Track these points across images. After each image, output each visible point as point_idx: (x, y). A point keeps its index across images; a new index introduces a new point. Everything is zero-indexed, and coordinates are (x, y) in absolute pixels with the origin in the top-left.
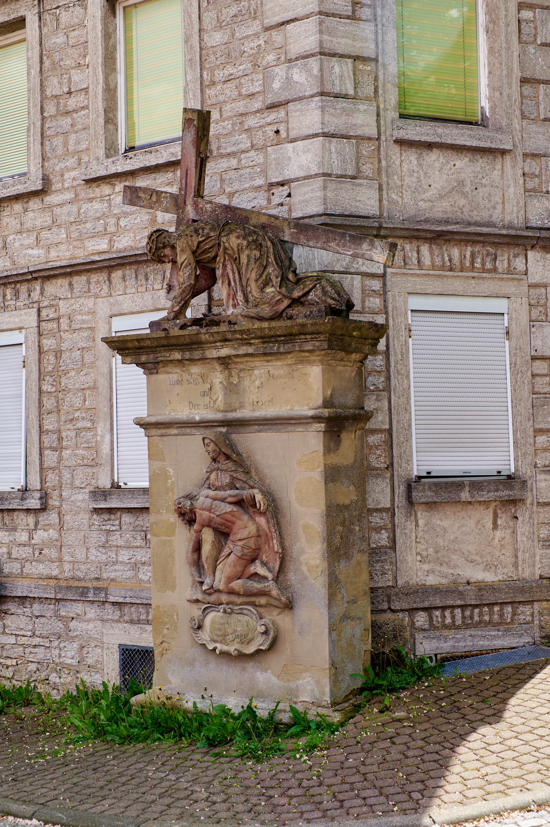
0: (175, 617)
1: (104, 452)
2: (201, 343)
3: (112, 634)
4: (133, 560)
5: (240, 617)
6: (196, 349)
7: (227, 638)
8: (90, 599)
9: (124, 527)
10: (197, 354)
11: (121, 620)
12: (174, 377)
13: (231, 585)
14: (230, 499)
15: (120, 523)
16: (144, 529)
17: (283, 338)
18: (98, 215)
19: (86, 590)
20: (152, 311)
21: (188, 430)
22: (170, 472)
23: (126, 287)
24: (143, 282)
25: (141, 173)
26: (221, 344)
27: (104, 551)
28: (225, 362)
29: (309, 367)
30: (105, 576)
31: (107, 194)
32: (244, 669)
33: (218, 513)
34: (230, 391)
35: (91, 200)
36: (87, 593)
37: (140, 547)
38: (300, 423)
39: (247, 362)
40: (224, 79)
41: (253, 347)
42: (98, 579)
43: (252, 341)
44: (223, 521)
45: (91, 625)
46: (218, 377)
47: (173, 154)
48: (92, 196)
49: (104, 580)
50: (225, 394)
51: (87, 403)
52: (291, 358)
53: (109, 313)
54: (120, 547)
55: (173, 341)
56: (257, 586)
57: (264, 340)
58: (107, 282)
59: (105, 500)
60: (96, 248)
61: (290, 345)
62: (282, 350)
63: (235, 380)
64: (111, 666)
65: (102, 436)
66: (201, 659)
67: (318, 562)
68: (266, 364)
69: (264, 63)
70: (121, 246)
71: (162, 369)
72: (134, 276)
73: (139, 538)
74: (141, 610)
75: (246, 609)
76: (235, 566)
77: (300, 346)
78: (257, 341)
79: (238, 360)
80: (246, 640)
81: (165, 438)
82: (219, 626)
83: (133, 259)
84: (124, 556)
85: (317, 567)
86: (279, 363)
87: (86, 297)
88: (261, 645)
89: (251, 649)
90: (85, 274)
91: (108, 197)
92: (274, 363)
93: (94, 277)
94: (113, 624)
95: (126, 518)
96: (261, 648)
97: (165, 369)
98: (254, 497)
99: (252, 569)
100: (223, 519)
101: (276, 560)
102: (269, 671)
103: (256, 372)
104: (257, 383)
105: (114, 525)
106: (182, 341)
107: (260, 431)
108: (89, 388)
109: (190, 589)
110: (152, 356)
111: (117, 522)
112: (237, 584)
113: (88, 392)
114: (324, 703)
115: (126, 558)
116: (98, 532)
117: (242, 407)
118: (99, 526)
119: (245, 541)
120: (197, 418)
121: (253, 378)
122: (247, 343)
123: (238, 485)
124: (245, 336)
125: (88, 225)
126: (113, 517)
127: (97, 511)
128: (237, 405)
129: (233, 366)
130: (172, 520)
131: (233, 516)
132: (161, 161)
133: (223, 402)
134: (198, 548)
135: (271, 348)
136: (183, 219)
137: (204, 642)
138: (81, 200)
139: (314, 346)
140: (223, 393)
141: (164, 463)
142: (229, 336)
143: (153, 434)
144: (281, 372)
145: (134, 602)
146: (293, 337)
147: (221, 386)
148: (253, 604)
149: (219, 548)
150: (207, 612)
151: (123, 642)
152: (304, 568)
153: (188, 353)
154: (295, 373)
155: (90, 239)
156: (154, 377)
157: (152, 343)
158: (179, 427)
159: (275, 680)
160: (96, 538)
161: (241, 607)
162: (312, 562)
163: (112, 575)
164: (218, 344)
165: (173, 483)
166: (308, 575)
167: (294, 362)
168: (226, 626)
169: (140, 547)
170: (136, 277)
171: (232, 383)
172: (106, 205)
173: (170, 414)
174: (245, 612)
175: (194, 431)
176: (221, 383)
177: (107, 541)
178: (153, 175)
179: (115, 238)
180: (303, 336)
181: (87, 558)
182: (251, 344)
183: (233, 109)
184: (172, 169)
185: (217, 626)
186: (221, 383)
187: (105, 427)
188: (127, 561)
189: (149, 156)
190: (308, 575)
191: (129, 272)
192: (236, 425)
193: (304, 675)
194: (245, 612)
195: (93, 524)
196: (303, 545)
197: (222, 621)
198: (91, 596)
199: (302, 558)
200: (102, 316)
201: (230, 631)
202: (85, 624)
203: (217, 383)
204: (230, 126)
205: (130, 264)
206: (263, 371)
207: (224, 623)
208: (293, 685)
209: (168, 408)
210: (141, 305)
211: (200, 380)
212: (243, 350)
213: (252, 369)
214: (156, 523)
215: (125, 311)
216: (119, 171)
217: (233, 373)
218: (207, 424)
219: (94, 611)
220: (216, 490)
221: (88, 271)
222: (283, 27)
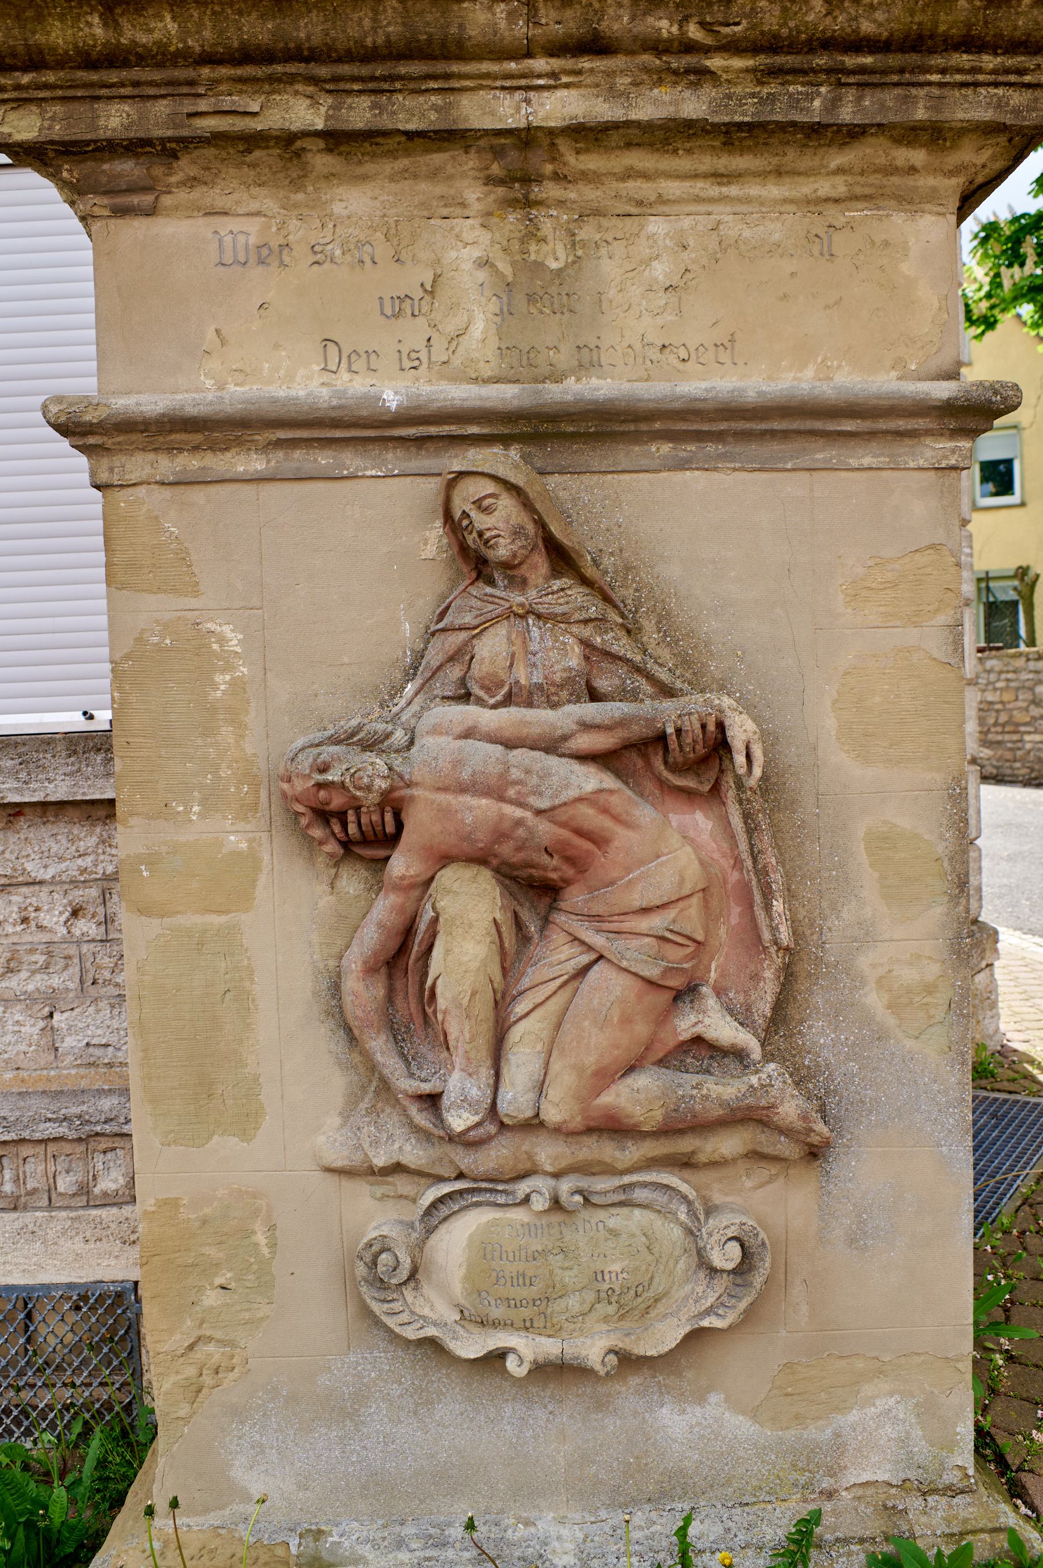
0: (261, 1238)
2: (456, 50)
5: (616, 1219)
6: (415, 86)
7: (558, 1306)
10: (412, 112)
12: (244, 231)
13: (607, 1099)
14: (585, 742)
17: (868, 60)
21: (323, 459)
22: (222, 640)
26: (556, 63)
29: (898, 218)
33: (544, 804)
34: (531, 298)
38: (873, 434)
39: (629, 174)
41: (709, 92)
43: (715, 62)
44: (565, 834)
46: (468, 243)
50: (506, 313)
52: (840, 171)
56: (723, 1089)
57: (780, 60)
61: (889, 97)
62: (847, 114)
63: (555, 255)
66: (395, 1390)
67: (933, 970)
68: (714, 191)
71: (182, 196)
75: (645, 1185)
76: (626, 1020)
78: (738, 63)
79: (592, 162)
80: (633, 1302)
81: (197, 495)
82: (520, 1266)
85: (929, 989)
86: (774, 190)
88: (709, 1312)
89: (664, 1336)
92: (754, 190)
96: (705, 1323)
97: (196, 194)
98: (721, 726)
99: (686, 1025)
100: (563, 825)
101: (756, 977)
102: (714, 1398)
103: (656, 226)
104: (661, 271)
107: (682, 465)
109: (337, 1121)
110: (162, 108)
112: (640, 1095)
114: (952, 1477)
119: (671, 913)
120: (392, 399)
121: (642, 249)
122: (688, 71)
123: (603, 684)
124: (694, 32)
128: (564, 358)
129: (551, 191)
130: (236, 841)
131: (605, 811)
133: (493, 342)
134: (404, 956)
135: (794, 102)
137: (431, 1331)
139: (1000, 105)
140: (494, 306)
141: (193, 602)
143: (134, 477)
144: (776, 229)
146: (914, 58)
147: (482, 275)
148: (685, 1163)
149: (514, 949)
150: (444, 1211)
152: (874, 1000)
153: (365, 102)
154: (838, 238)
156: (136, 228)
157: (184, 33)
158: (279, 444)
159: (739, 1426)
161: (627, 1179)
162: (908, 975)
164: (540, 64)
165: (237, 686)
166: (891, 1021)
167: (841, 190)
168: (556, 1261)
171: (539, 266)
173: (221, 387)
174: (640, 1195)
175: (351, 460)
176: (485, 263)
180: (964, 59)
182: (701, 75)
185: (511, 1269)
186: (485, 263)
190: (891, 1021)
192: (574, 436)
193: (868, 1390)
194: (640, 1195)
196: (868, 912)
197: (536, 1245)
199: (864, 962)
201: (568, 1277)
203: (467, 266)
206: (687, 222)
207: (544, 1253)
208: (820, 1433)
209: (213, 364)
211: (382, 250)
212: (655, 102)
213: (643, 207)
214: (152, 861)
217: (547, 227)
218: (433, 430)
220: (508, 701)
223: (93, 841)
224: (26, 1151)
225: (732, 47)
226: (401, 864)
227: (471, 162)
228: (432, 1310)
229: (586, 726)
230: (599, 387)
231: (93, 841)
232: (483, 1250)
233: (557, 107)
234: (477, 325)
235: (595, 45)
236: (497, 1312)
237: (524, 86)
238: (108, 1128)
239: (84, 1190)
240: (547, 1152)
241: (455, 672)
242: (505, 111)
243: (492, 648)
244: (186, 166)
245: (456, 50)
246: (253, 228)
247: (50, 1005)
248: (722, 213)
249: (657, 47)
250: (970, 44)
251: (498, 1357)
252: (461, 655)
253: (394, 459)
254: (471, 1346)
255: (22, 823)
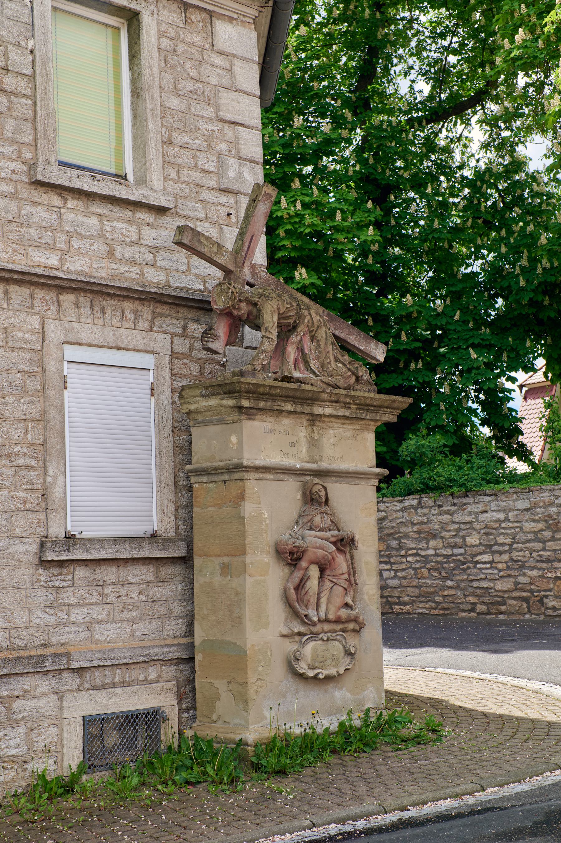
1: (57, 495)
3: (74, 706)
4: (87, 619)
8: (48, 669)
9: (77, 582)
10: (307, 409)
11: (81, 688)
15: (73, 577)
16: (101, 583)
18: (44, 224)
19: (42, 659)
20: (111, 348)
21: (282, 476)
23: (80, 315)
24: (99, 314)
25: (98, 198)
27: (52, 611)
28: (314, 419)
30: (54, 640)
31: (57, 205)
32: (326, 691)
35: (35, 204)
36: (43, 662)
37: (96, 604)
40: (180, 144)
42: (44, 646)
45: (43, 702)
46: (303, 433)
47: (144, 196)
48: (36, 199)
49: (53, 645)
50: (309, 448)
51: (29, 437)
53: (62, 338)
54: (73, 605)
55: (298, 394)
58: (56, 303)
59: (69, 551)
60: (43, 260)
64: (73, 745)
65: (55, 478)
69: (218, 148)
70: (72, 268)
71: (259, 417)
72: (88, 305)
73: (95, 593)
74: (106, 673)
77: (380, 417)
79: (326, 419)
81: (261, 482)
83: (98, 288)
84: (78, 615)
86: (350, 427)
87: (28, 314)
90: (28, 286)
91: (57, 210)
93: (40, 293)
94: (76, 694)
95: (81, 572)
103: (331, 432)
104: (332, 441)
105: (65, 581)
106: (306, 395)
107: (336, 482)
108: (32, 420)
110: (269, 403)
111: (70, 577)
113: (30, 424)
115: (80, 618)
116: (45, 590)
117: (321, 460)
118: (47, 582)
125: (33, 231)
126: (64, 571)
127: (43, 563)
132: (132, 198)
136: (239, 277)
138: (23, 199)
142: (342, 399)
145: (102, 664)
151: (87, 713)
152: (366, 597)
155: (36, 249)
160: (42, 596)
163: (63, 639)
169: (96, 604)
170: (92, 307)
172: (54, 216)
175: (286, 477)
176: (305, 437)
177: (56, 600)
178: (110, 206)
179: (66, 257)
181: (30, 621)
183: (190, 176)
184: (132, 208)
187: (57, 467)
188: (82, 621)
189: (118, 186)
191: (85, 300)
195: (39, 581)
198: (48, 665)
199: (364, 589)
200: (55, 340)
201: (328, 656)
202: (35, 700)
204: (187, 191)
205: (85, 291)
208: (361, 697)
210: (102, 339)
215: (83, 342)
216: (85, 189)
219: (47, 683)
221: (33, 284)
222: (233, 125)
223: (145, 570)
224: (133, 667)
225: (355, 404)
226: (304, 564)
227: (307, 417)
228: (302, 667)
229: (332, 536)
230: (325, 465)
231: (145, 570)
232: (315, 650)
233: (328, 411)
234: (304, 449)
235: (336, 402)
236: (317, 664)
237: (324, 407)
238: (156, 658)
239: (146, 679)
240: (327, 627)
241: (309, 524)
242: (318, 410)
243: (317, 519)
244: (263, 412)
245: (317, 400)
246: (270, 424)
247: (133, 621)
248: (341, 430)
249: (345, 403)
250: (387, 407)
251: (317, 674)
252: (311, 520)
253: (293, 478)
254: (311, 674)
255: (128, 564)
